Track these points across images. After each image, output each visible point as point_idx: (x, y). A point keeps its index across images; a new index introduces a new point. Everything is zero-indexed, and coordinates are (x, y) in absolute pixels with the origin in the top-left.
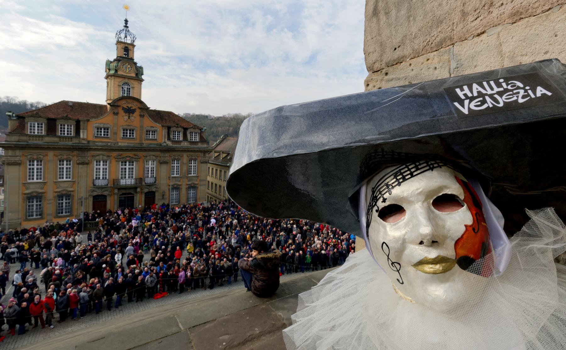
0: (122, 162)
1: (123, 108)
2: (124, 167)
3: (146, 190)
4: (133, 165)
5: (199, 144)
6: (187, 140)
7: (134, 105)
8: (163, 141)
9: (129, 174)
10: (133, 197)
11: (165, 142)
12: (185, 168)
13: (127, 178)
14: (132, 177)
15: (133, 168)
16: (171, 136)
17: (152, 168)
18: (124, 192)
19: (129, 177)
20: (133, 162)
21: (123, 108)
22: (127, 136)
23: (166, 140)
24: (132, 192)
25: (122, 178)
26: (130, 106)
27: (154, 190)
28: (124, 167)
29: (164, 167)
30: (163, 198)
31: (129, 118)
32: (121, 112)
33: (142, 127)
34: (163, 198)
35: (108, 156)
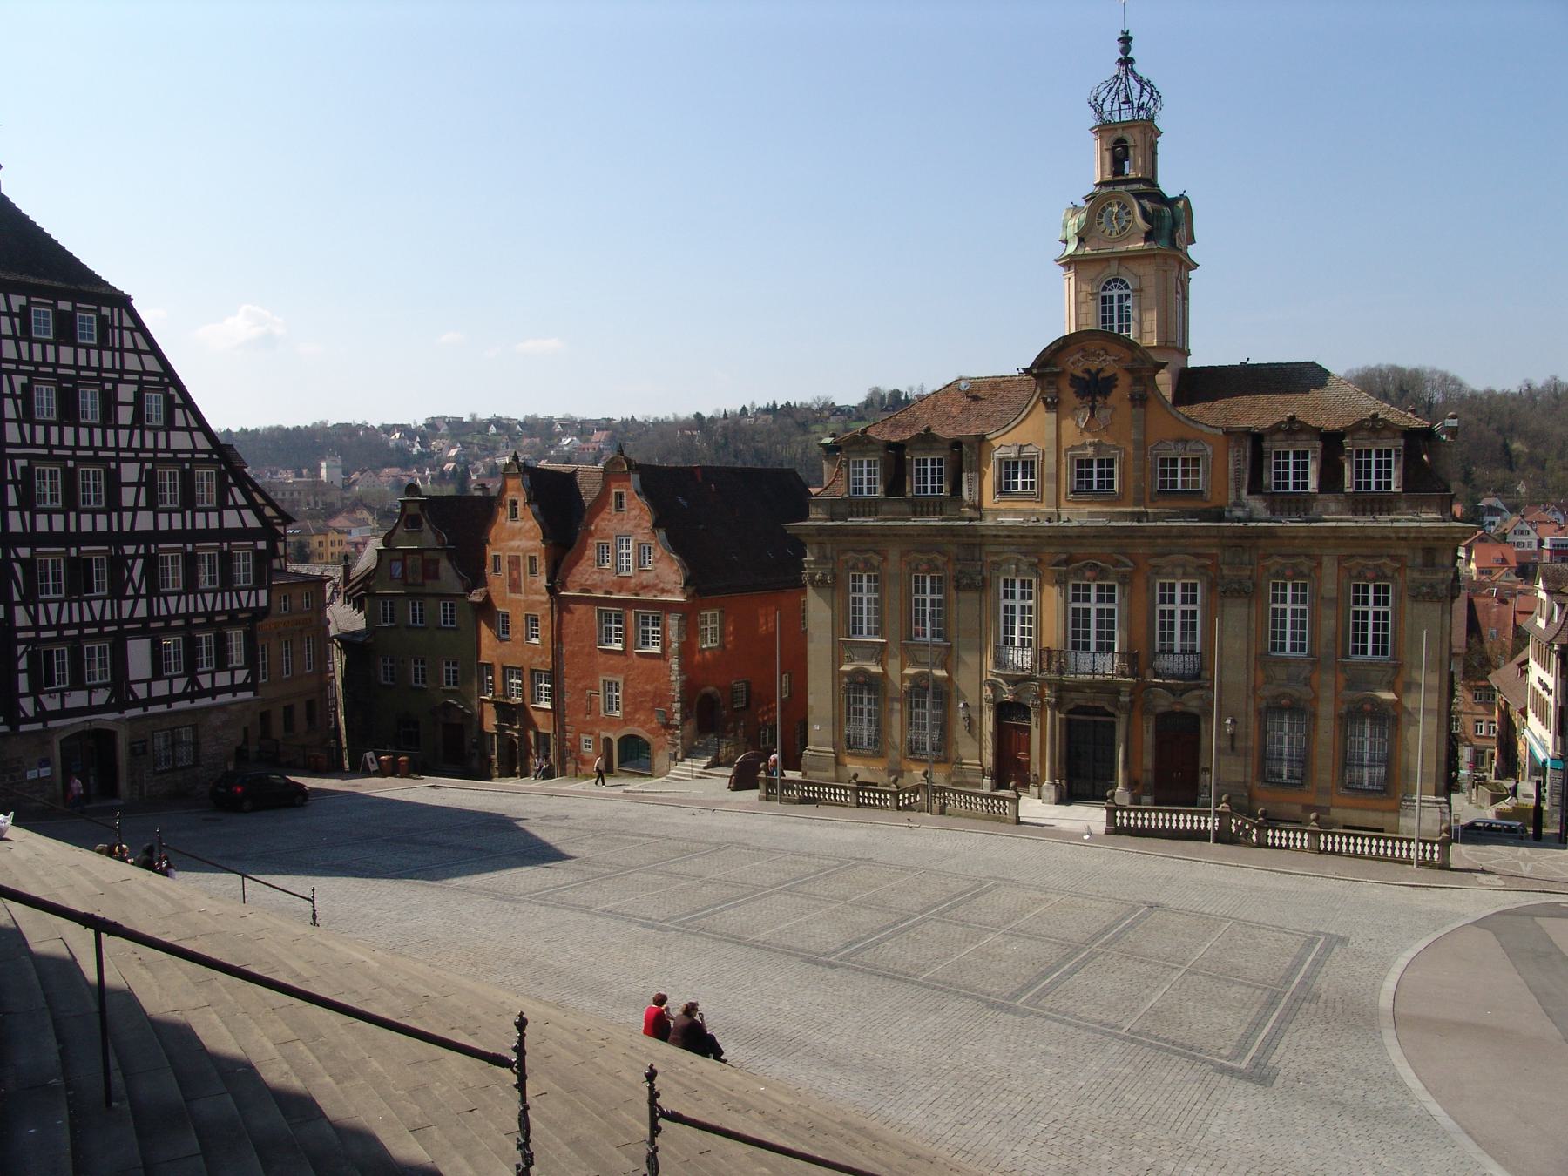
0: (1076, 588)
1: (1075, 381)
2: (1081, 605)
3: (1164, 702)
4: (1111, 599)
5: (1403, 505)
6: (1342, 491)
7: (1107, 364)
8: (1232, 498)
9: (1100, 635)
10: (1112, 726)
11: (1238, 504)
12: (1329, 624)
13: (1093, 648)
14: (1111, 647)
15: (1111, 612)
16: (1269, 478)
17: (1189, 616)
18: (1078, 699)
19: (1100, 647)
20: (1111, 588)
21: (1075, 381)
22: (1090, 484)
23: (1244, 492)
24: (1110, 709)
25: (1075, 646)
26: (1094, 365)
27: (1192, 702)
28: (1081, 605)
29: (1236, 614)
30: (1233, 748)
31: (1092, 415)
32: (1068, 394)
33: (1141, 446)
34: (1233, 748)
35: (1032, 565)
